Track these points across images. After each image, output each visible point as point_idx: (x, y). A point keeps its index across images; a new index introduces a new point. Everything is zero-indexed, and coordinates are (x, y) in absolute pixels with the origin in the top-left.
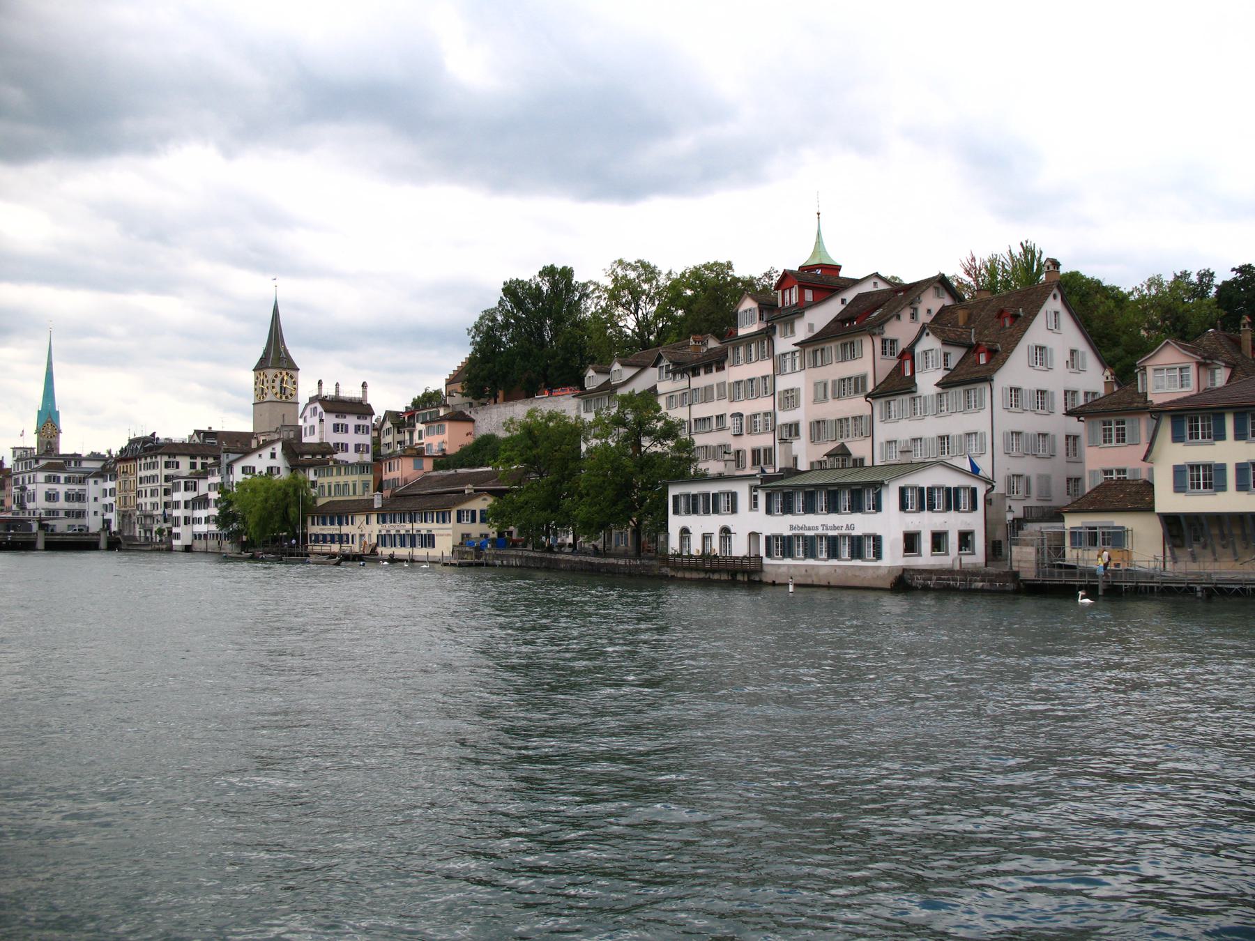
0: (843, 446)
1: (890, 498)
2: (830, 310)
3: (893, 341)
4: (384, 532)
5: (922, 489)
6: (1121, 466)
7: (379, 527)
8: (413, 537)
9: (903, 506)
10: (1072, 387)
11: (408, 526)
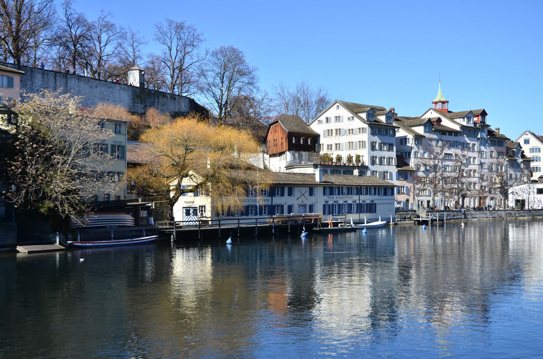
7: (326, 198)
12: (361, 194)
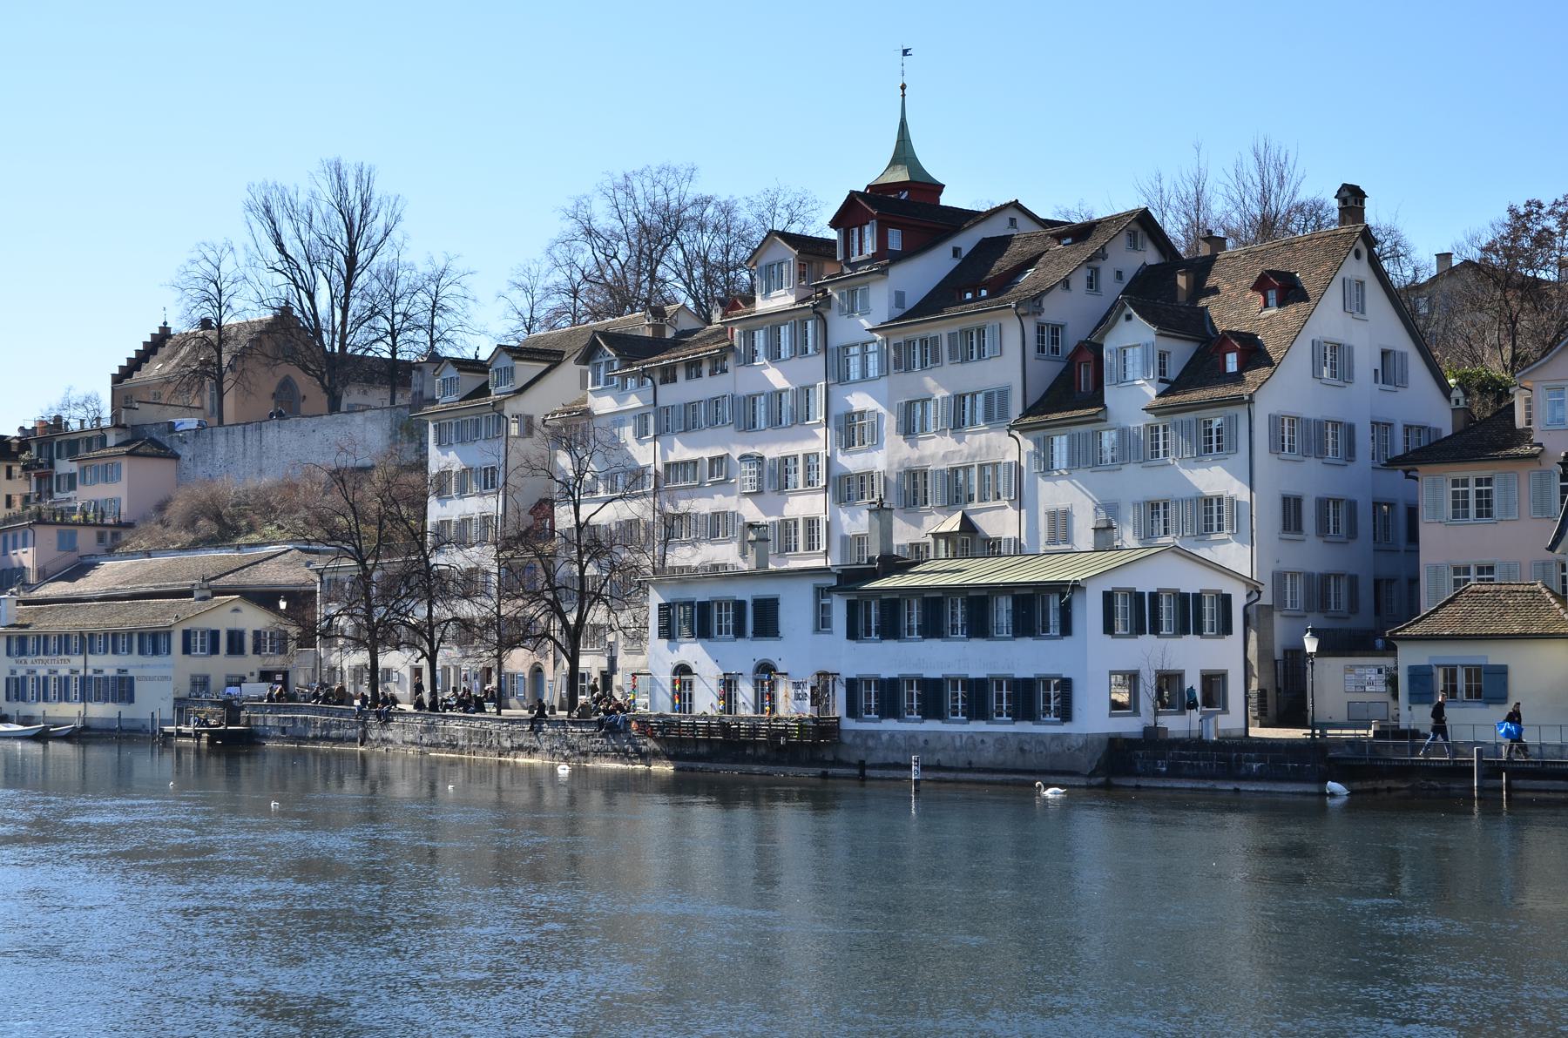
1: (1090, 612)
2: (933, 267)
3: (1056, 329)
4: (20, 673)
5: (1139, 597)
6: (1486, 560)
8: (85, 680)
9: (1109, 628)
10: (1382, 416)
11: (77, 661)
12: (91, 652)
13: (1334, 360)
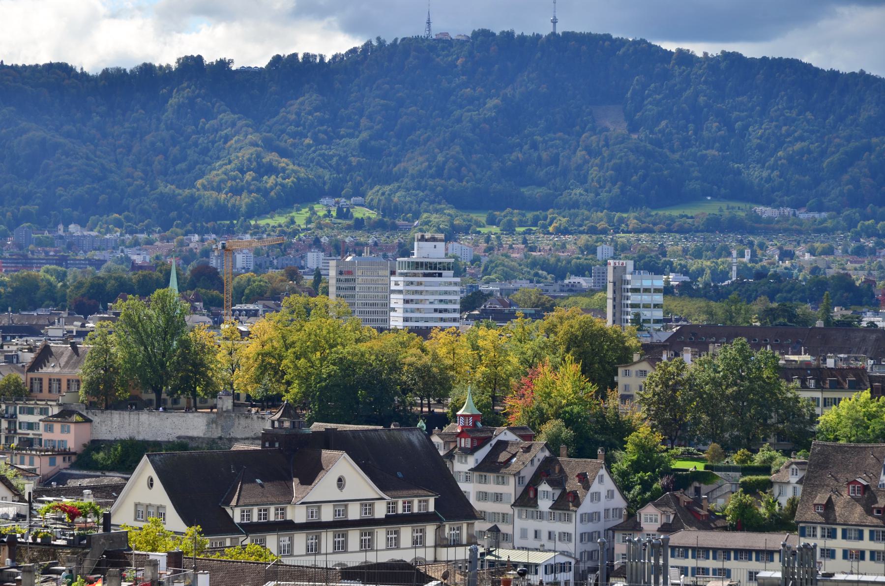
0: (496, 527)
1: (541, 570)
9: (546, 573)
10: (607, 507)
13: (596, 497)
